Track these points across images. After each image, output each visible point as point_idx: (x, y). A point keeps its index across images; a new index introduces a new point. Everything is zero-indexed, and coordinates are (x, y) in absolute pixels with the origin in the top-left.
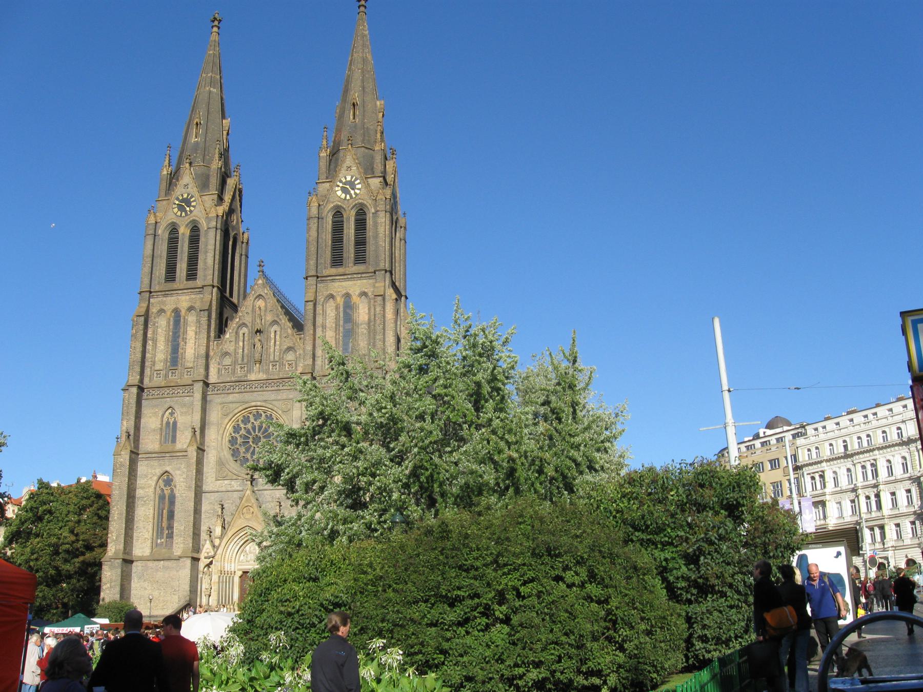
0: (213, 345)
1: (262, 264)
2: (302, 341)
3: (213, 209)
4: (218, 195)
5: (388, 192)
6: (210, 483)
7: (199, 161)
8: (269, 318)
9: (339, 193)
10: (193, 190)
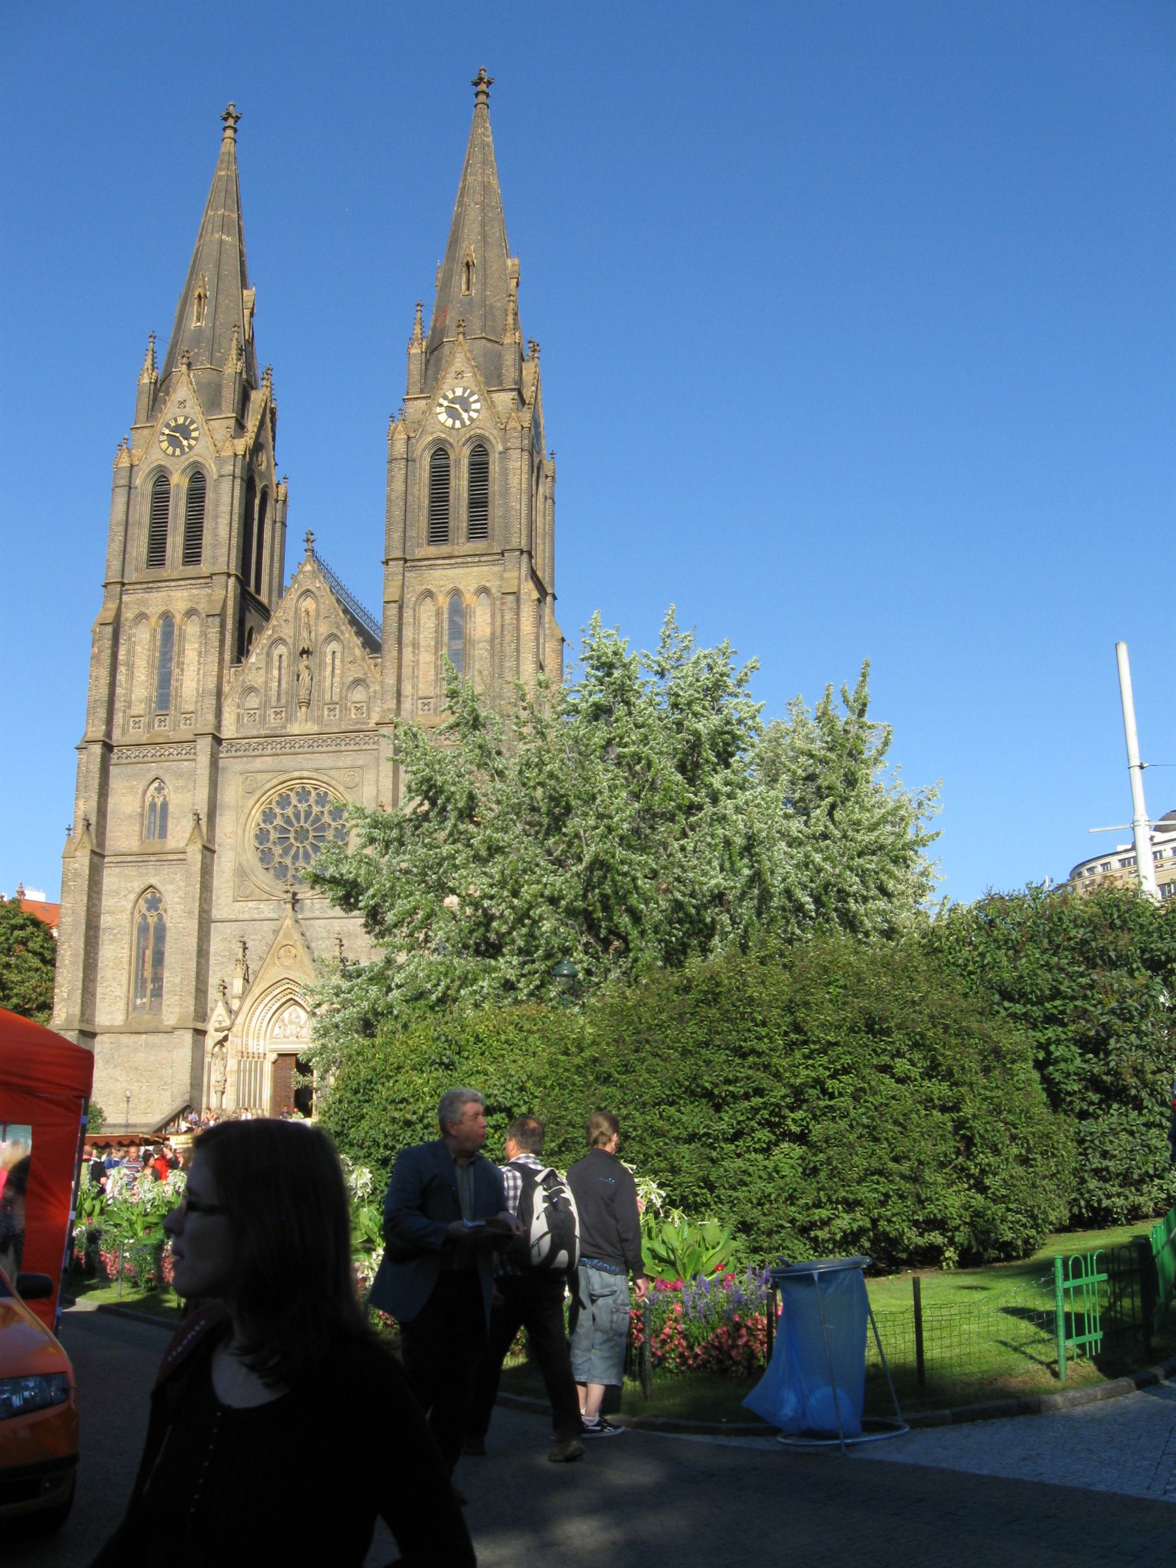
0: (229, 673)
1: (312, 538)
2: (379, 669)
3: (227, 444)
4: (237, 420)
5: (526, 416)
6: (223, 906)
7: (203, 363)
8: (324, 629)
9: (443, 417)
10: (194, 410)
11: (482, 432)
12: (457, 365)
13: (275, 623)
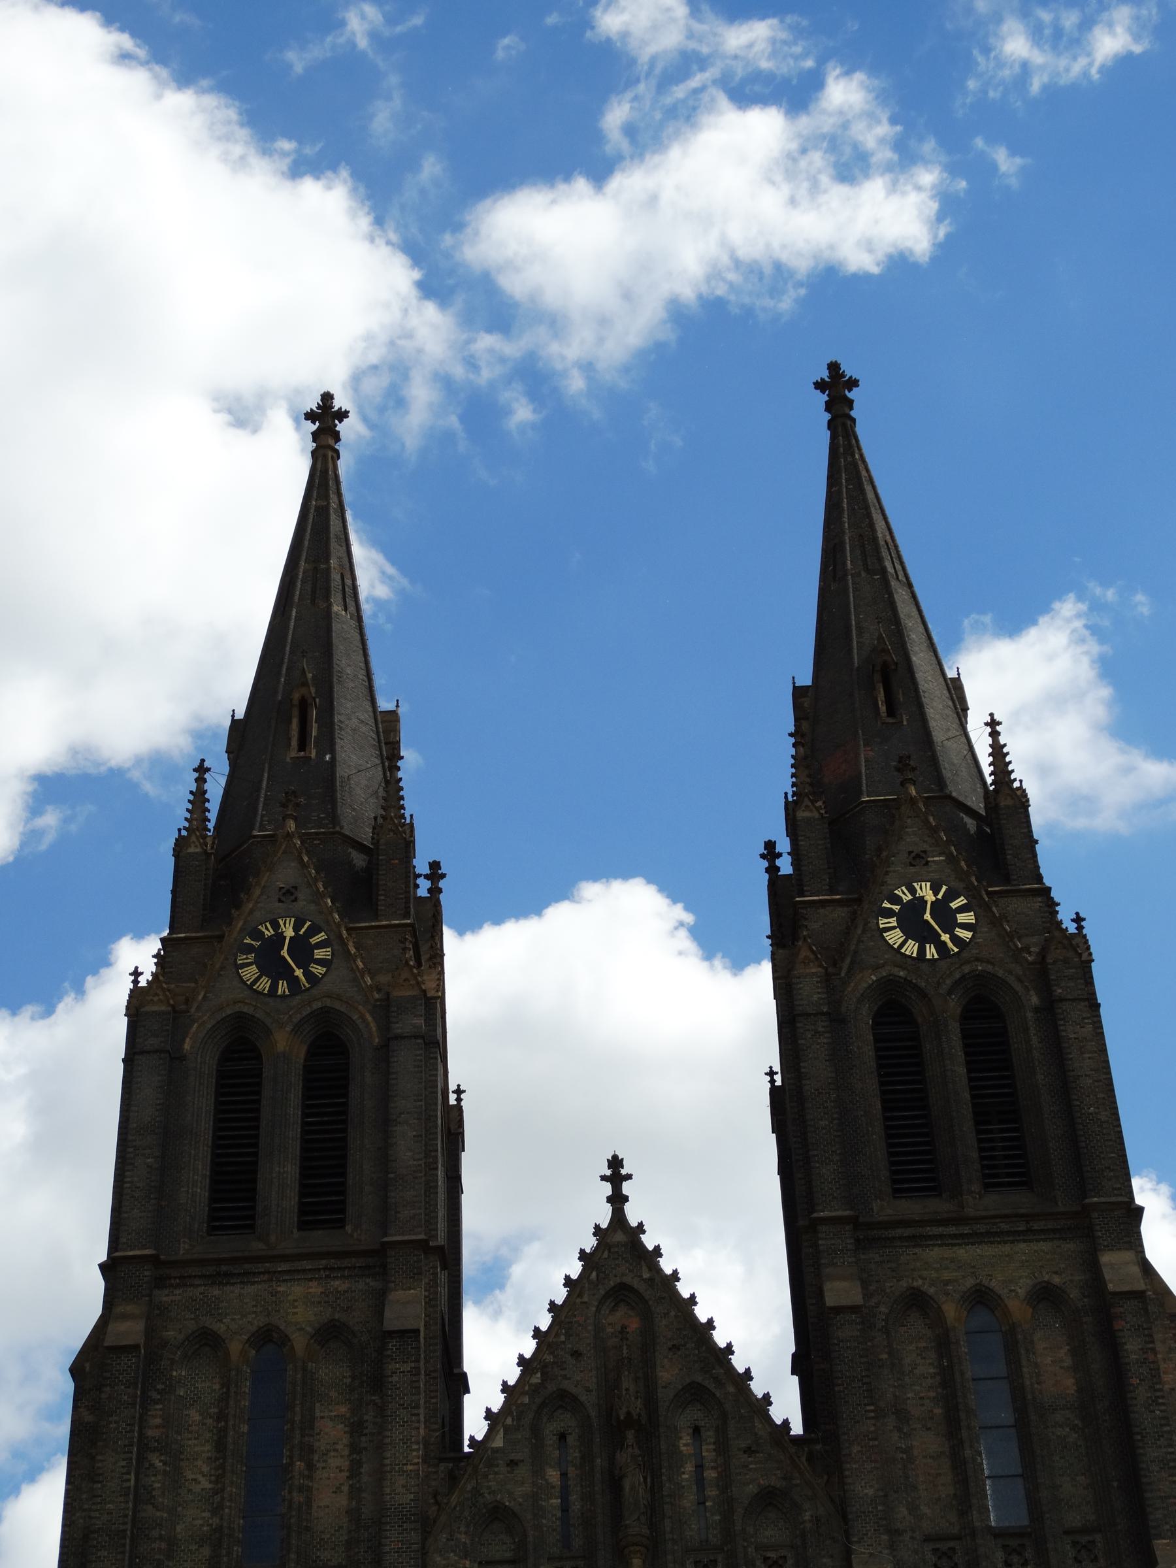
9: (895, 937)
11: (990, 968)
13: (550, 1358)
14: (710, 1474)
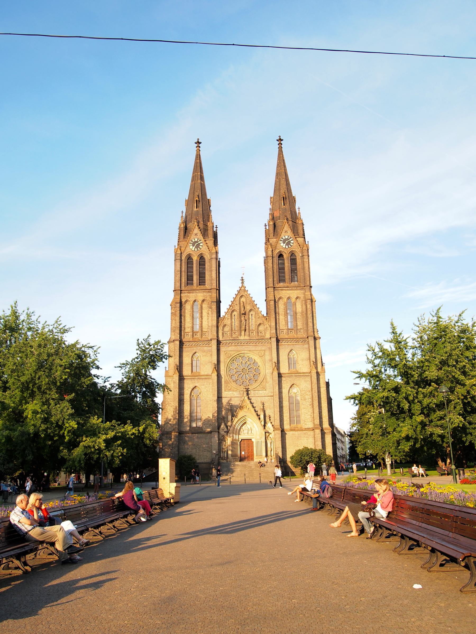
12: (285, 229)
13: (233, 305)
14: (253, 321)
